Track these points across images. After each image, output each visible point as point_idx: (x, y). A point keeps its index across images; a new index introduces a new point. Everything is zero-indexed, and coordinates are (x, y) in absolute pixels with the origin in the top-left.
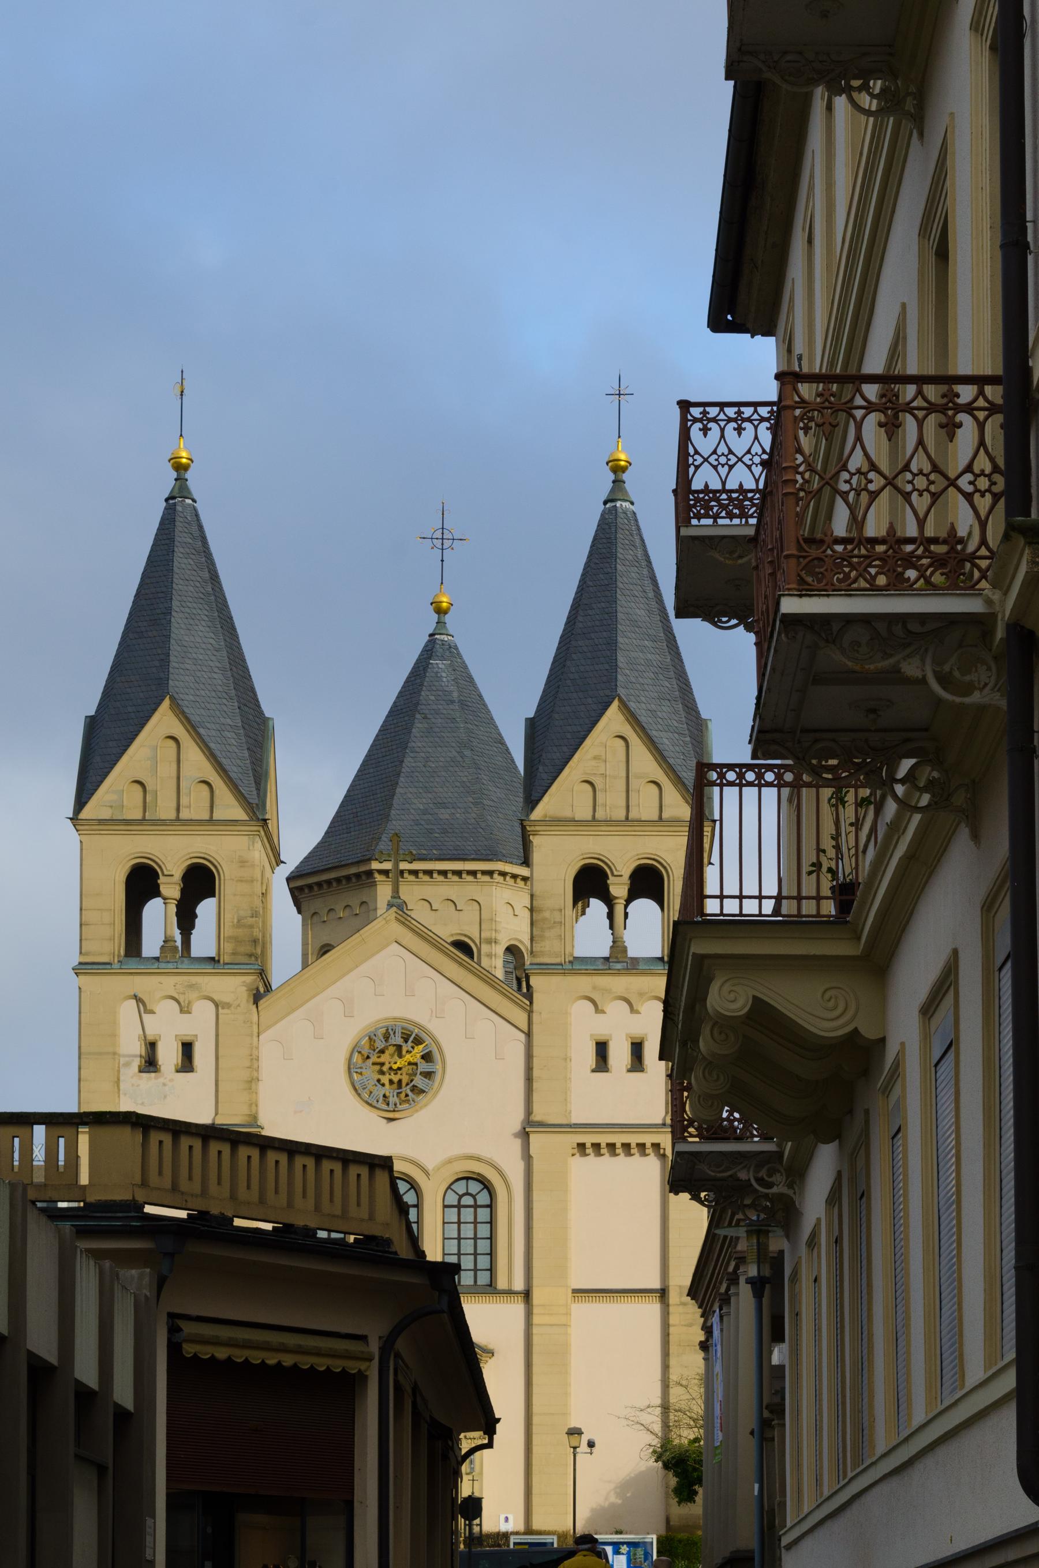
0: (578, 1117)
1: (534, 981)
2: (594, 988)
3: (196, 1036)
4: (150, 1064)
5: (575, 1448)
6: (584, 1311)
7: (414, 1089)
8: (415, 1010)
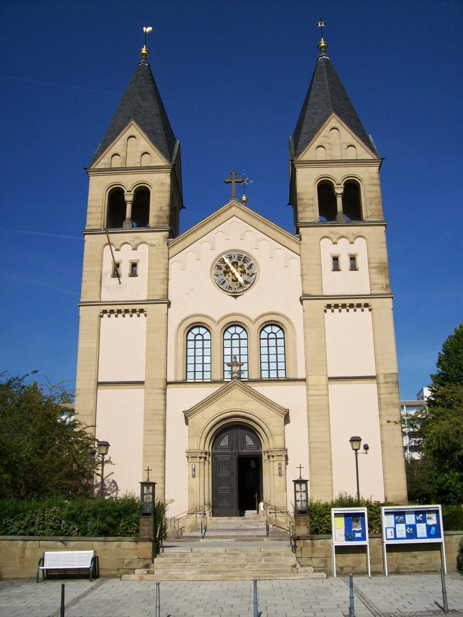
1: (301, 230)
2: (331, 232)
4: (116, 274)
6: (334, 387)
8: (246, 247)
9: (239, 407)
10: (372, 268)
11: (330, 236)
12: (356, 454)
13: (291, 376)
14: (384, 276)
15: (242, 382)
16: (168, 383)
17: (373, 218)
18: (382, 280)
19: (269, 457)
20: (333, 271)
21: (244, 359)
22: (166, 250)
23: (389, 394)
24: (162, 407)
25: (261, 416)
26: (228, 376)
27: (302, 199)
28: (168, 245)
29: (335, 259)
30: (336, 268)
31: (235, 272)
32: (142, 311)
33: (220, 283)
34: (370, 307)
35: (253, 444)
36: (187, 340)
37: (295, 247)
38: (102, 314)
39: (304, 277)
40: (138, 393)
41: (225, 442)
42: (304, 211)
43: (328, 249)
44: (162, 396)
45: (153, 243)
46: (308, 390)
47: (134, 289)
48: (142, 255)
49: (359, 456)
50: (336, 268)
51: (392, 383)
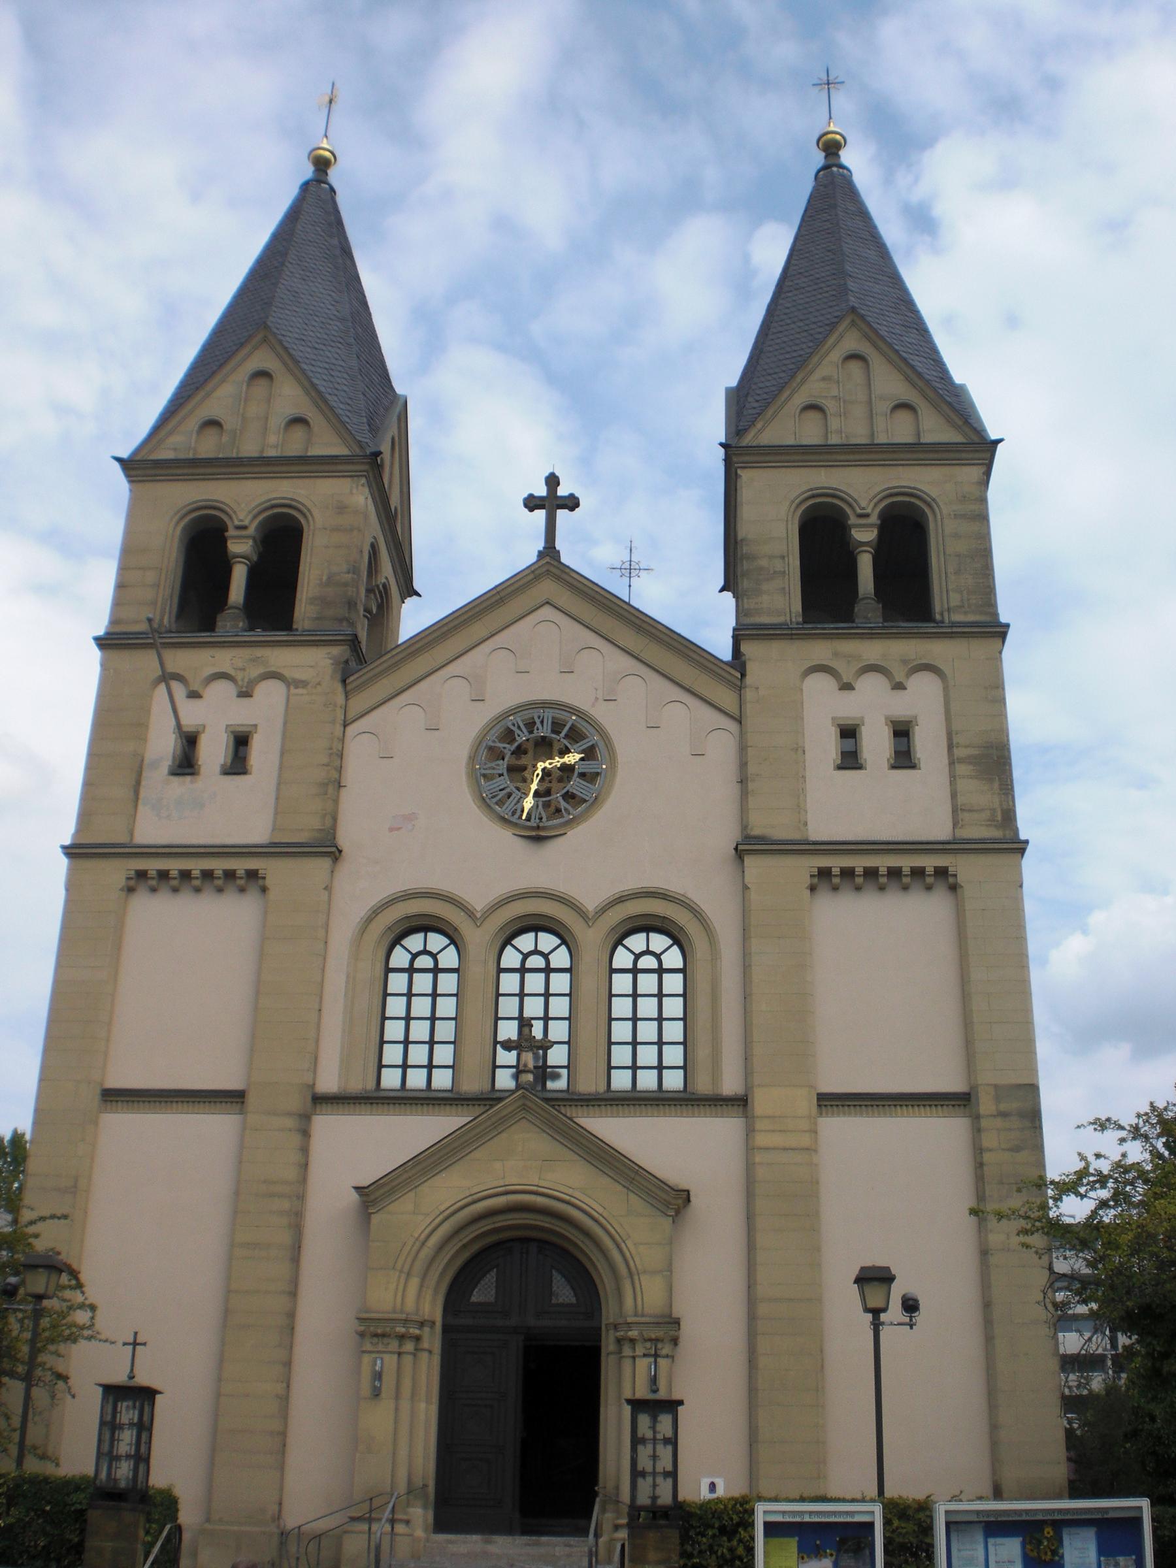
0: (819, 830)
3: (256, 726)
4: (186, 763)
5: (876, 1312)
7: (569, 797)
8: (578, 693)
9: (533, 1179)
10: (961, 761)
11: (834, 664)
12: (877, 1326)
13: (703, 1086)
14: (996, 785)
15: (546, 1100)
17: (966, 613)
19: (619, 1341)
20: (840, 768)
21: (558, 1031)
22: (340, 699)
23: (1010, 1150)
24: (291, 1174)
25: (601, 1210)
26: (504, 1080)
27: (752, 558)
28: (344, 681)
29: (849, 732)
30: (850, 760)
32: (252, 875)
33: (494, 800)
34: (951, 880)
35: (574, 1300)
36: (388, 970)
38: (132, 883)
39: (751, 786)
40: (218, 1126)
41: (484, 1293)
43: (822, 705)
44: (296, 1139)
45: (298, 675)
46: (750, 1131)
47: (234, 812)
48: (265, 711)
49: (885, 1332)
50: (850, 760)
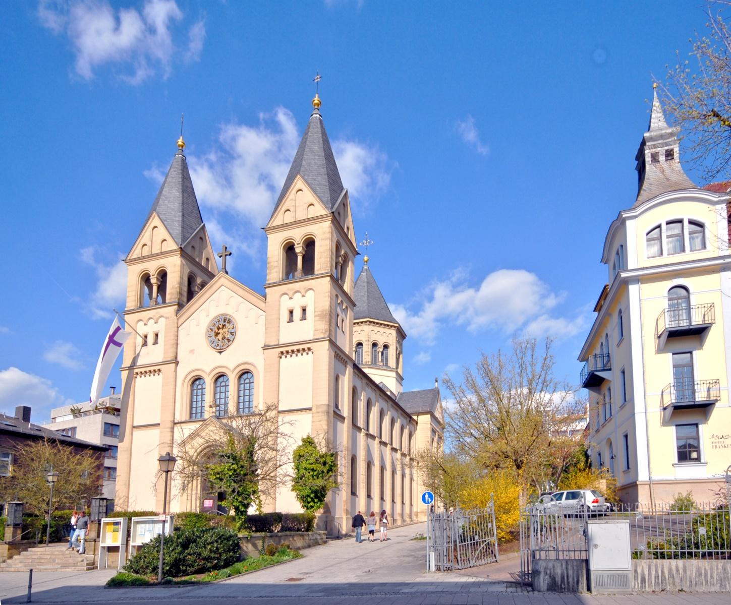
2: (288, 289)
8: (229, 311)
14: (324, 322)
16: (175, 424)
18: (323, 326)
22: (176, 321)
27: (270, 263)
30: (291, 320)
31: (222, 332)
37: (261, 304)
40: (155, 432)
42: (270, 273)
43: (286, 303)
44: (170, 434)
51: (322, 412)
